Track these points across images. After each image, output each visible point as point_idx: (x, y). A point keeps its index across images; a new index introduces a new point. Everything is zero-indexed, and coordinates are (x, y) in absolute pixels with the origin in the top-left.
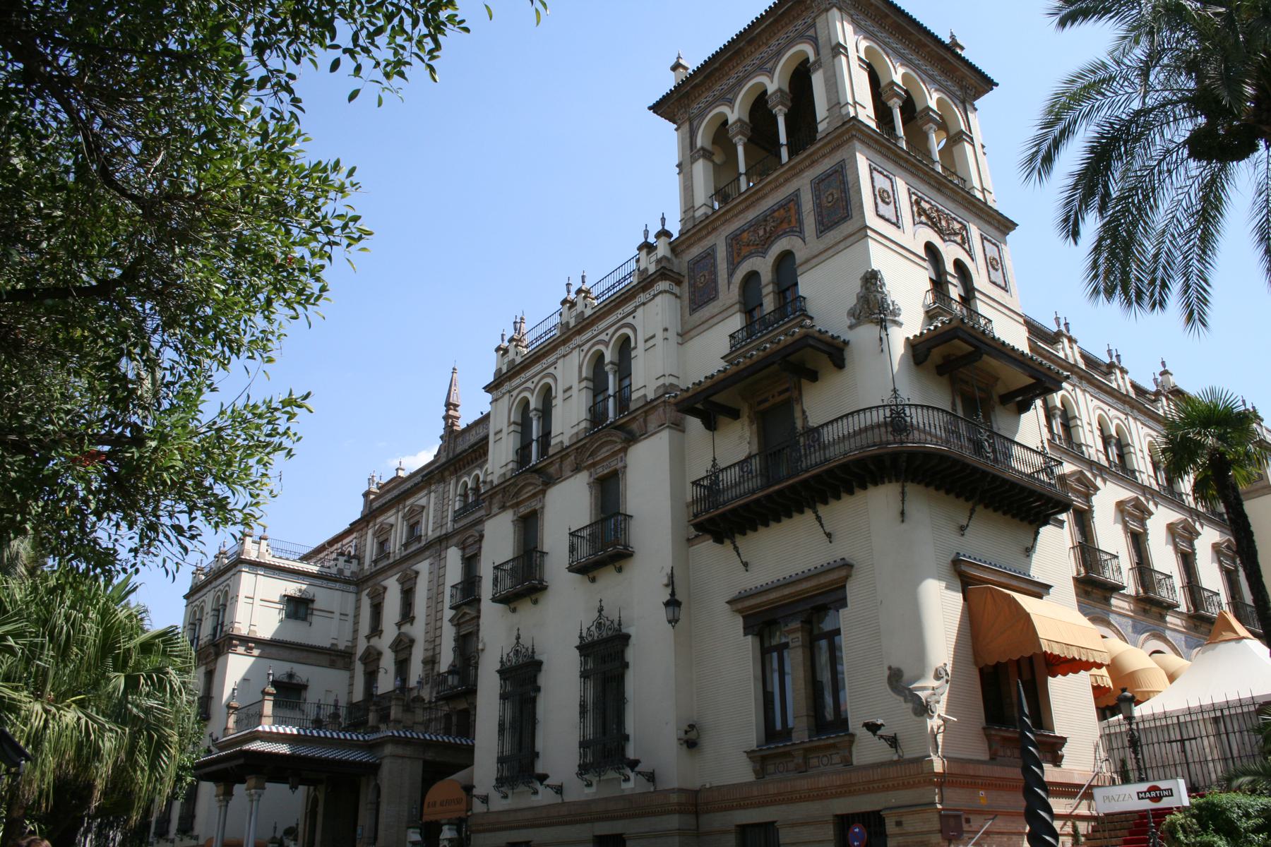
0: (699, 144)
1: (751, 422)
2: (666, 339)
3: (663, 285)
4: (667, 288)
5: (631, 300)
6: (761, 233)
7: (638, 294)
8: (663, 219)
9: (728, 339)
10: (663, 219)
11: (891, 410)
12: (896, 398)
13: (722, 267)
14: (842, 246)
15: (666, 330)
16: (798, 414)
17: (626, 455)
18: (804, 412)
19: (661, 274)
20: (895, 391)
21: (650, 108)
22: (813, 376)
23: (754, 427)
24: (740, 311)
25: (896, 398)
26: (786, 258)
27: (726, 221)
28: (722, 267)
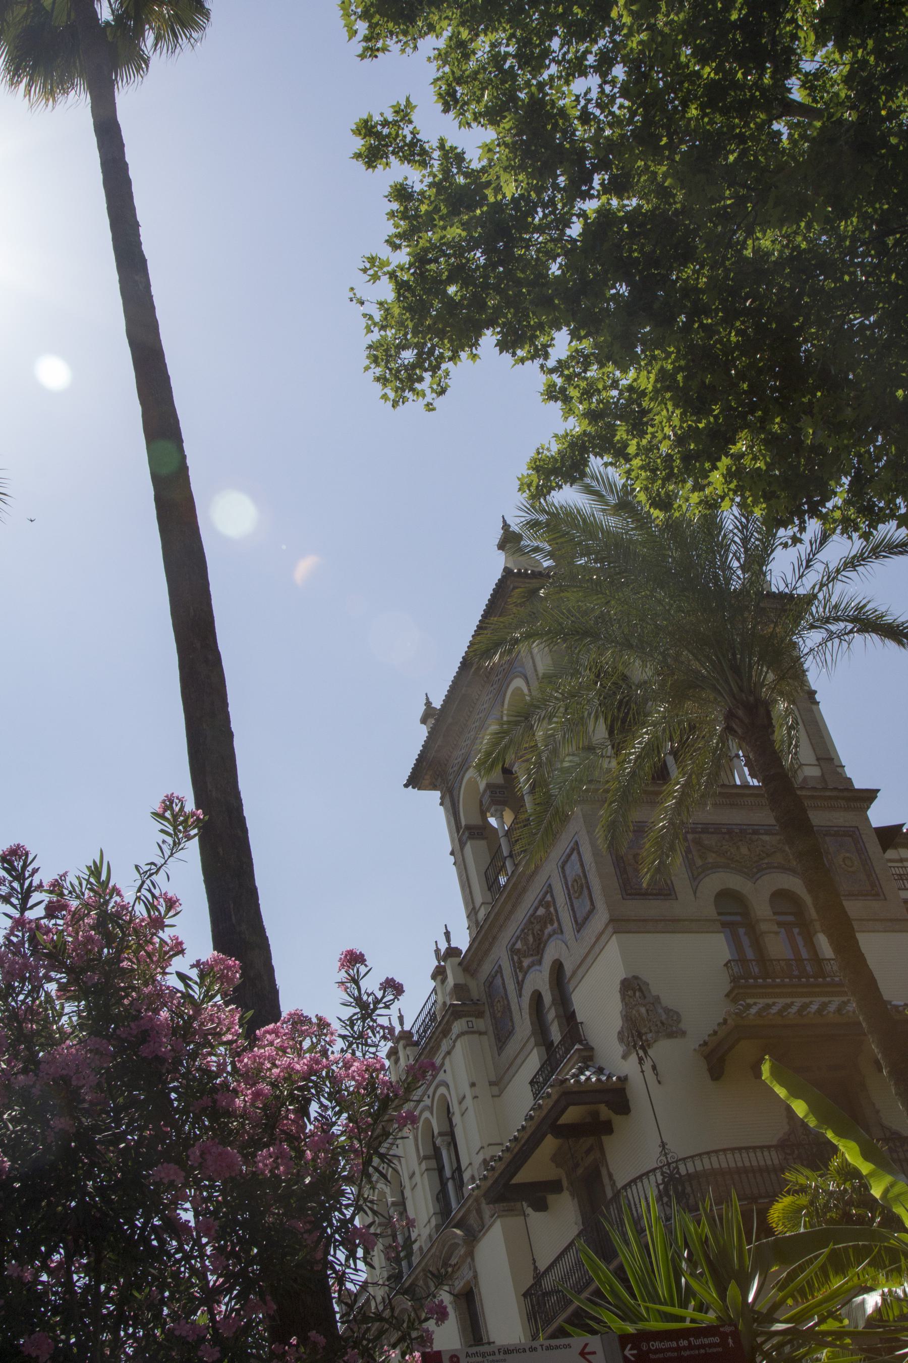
0: (463, 823)
1: (572, 1195)
2: (476, 1097)
3: (458, 1026)
4: (465, 1028)
5: (438, 1050)
6: (531, 939)
7: (441, 1040)
8: (447, 934)
9: (529, 1087)
10: (447, 934)
11: (663, 1174)
12: (666, 1154)
13: (511, 987)
14: (597, 949)
15: (473, 1085)
16: (606, 1180)
17: (473, 1259)
18: (610, 1176)
19: (452, 1014)
20: (663, 1145)
21: (406, 786)
22: (607, 1128)
23: (576, 1199)
24: (537, 1045)
25: (666, 1154)
26: (558, 968)
27: (501, 926)
28: (511, 987)
